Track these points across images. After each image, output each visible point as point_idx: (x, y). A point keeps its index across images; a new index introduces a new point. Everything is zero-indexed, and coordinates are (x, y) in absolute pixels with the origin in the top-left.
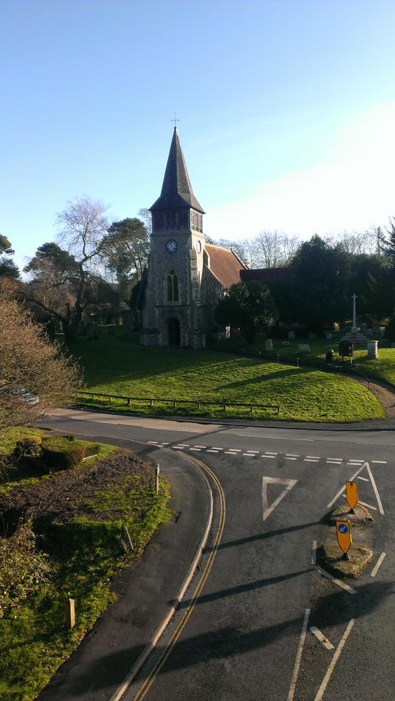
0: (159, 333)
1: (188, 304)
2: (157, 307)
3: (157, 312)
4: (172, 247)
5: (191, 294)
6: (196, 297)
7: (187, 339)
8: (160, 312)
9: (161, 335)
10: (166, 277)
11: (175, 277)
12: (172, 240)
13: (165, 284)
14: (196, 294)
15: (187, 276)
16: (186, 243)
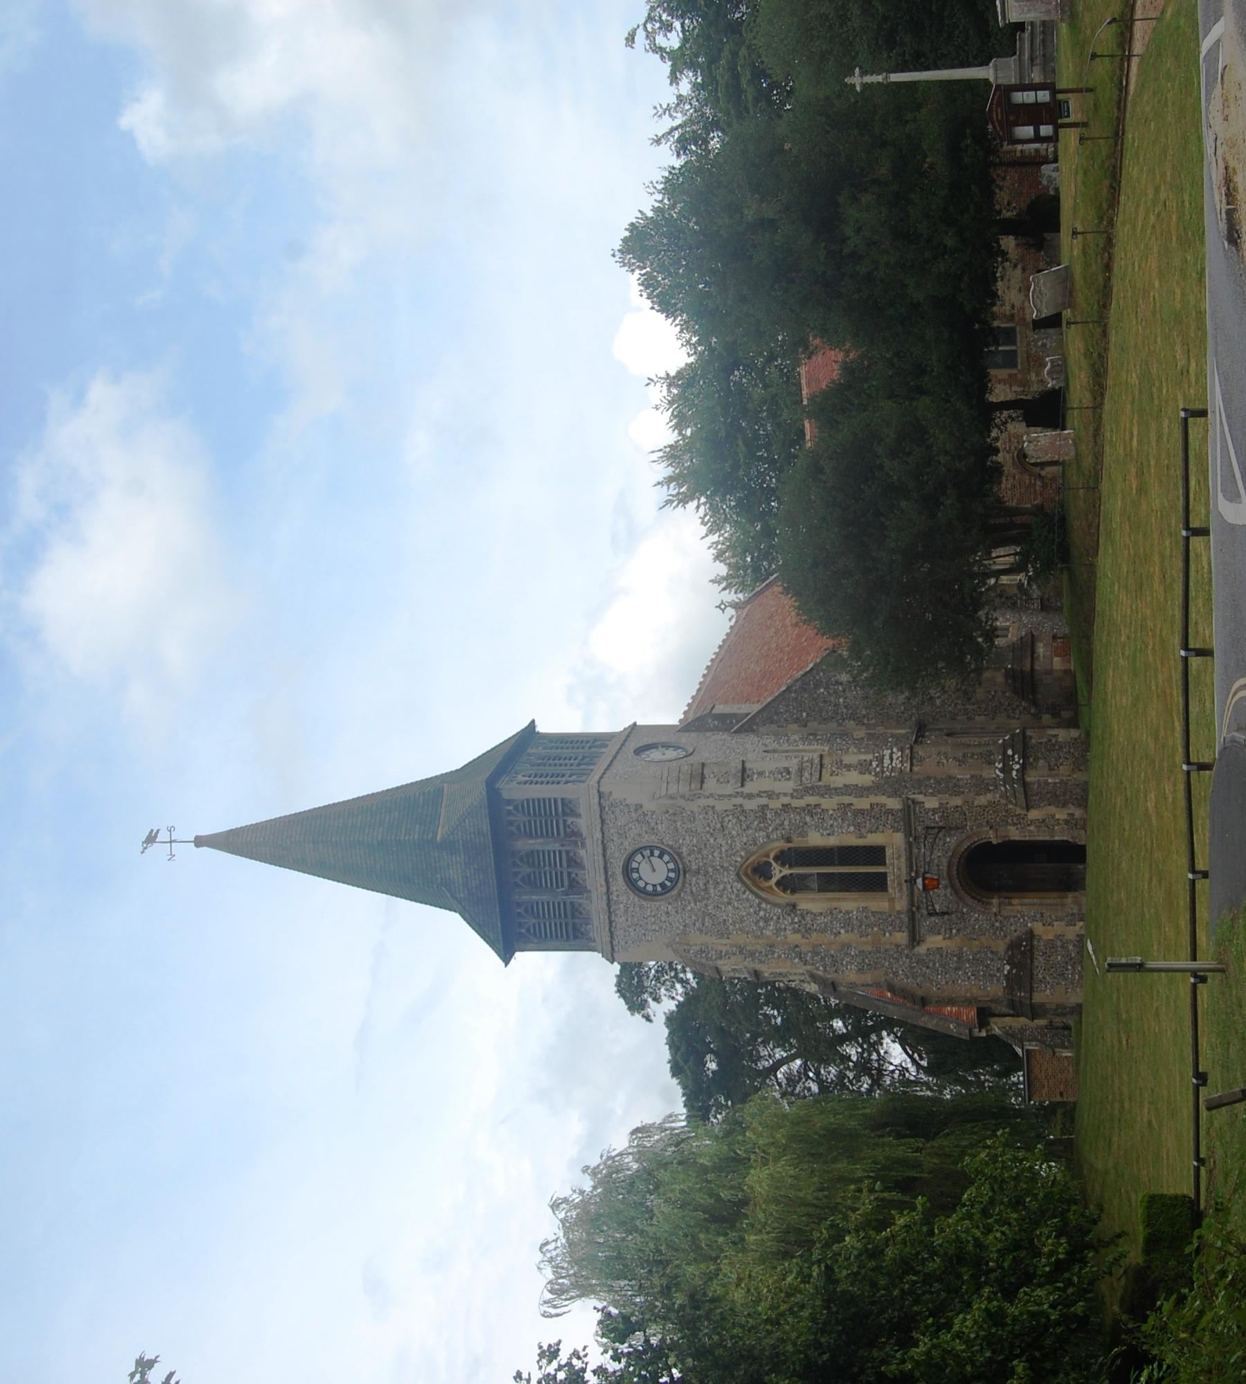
0: (1031, 935)
1: (894, 804)
2: (915, 940)
3: (934, 941)
4: (653, 872)
5: (847, 789)
6: (864, 767)
7: (1052, 809)
9: (1038, 928)
10: (787, 897)
11: (782, 858)
12: (627, 871)
14: (849, 767)
15: (775, 804)
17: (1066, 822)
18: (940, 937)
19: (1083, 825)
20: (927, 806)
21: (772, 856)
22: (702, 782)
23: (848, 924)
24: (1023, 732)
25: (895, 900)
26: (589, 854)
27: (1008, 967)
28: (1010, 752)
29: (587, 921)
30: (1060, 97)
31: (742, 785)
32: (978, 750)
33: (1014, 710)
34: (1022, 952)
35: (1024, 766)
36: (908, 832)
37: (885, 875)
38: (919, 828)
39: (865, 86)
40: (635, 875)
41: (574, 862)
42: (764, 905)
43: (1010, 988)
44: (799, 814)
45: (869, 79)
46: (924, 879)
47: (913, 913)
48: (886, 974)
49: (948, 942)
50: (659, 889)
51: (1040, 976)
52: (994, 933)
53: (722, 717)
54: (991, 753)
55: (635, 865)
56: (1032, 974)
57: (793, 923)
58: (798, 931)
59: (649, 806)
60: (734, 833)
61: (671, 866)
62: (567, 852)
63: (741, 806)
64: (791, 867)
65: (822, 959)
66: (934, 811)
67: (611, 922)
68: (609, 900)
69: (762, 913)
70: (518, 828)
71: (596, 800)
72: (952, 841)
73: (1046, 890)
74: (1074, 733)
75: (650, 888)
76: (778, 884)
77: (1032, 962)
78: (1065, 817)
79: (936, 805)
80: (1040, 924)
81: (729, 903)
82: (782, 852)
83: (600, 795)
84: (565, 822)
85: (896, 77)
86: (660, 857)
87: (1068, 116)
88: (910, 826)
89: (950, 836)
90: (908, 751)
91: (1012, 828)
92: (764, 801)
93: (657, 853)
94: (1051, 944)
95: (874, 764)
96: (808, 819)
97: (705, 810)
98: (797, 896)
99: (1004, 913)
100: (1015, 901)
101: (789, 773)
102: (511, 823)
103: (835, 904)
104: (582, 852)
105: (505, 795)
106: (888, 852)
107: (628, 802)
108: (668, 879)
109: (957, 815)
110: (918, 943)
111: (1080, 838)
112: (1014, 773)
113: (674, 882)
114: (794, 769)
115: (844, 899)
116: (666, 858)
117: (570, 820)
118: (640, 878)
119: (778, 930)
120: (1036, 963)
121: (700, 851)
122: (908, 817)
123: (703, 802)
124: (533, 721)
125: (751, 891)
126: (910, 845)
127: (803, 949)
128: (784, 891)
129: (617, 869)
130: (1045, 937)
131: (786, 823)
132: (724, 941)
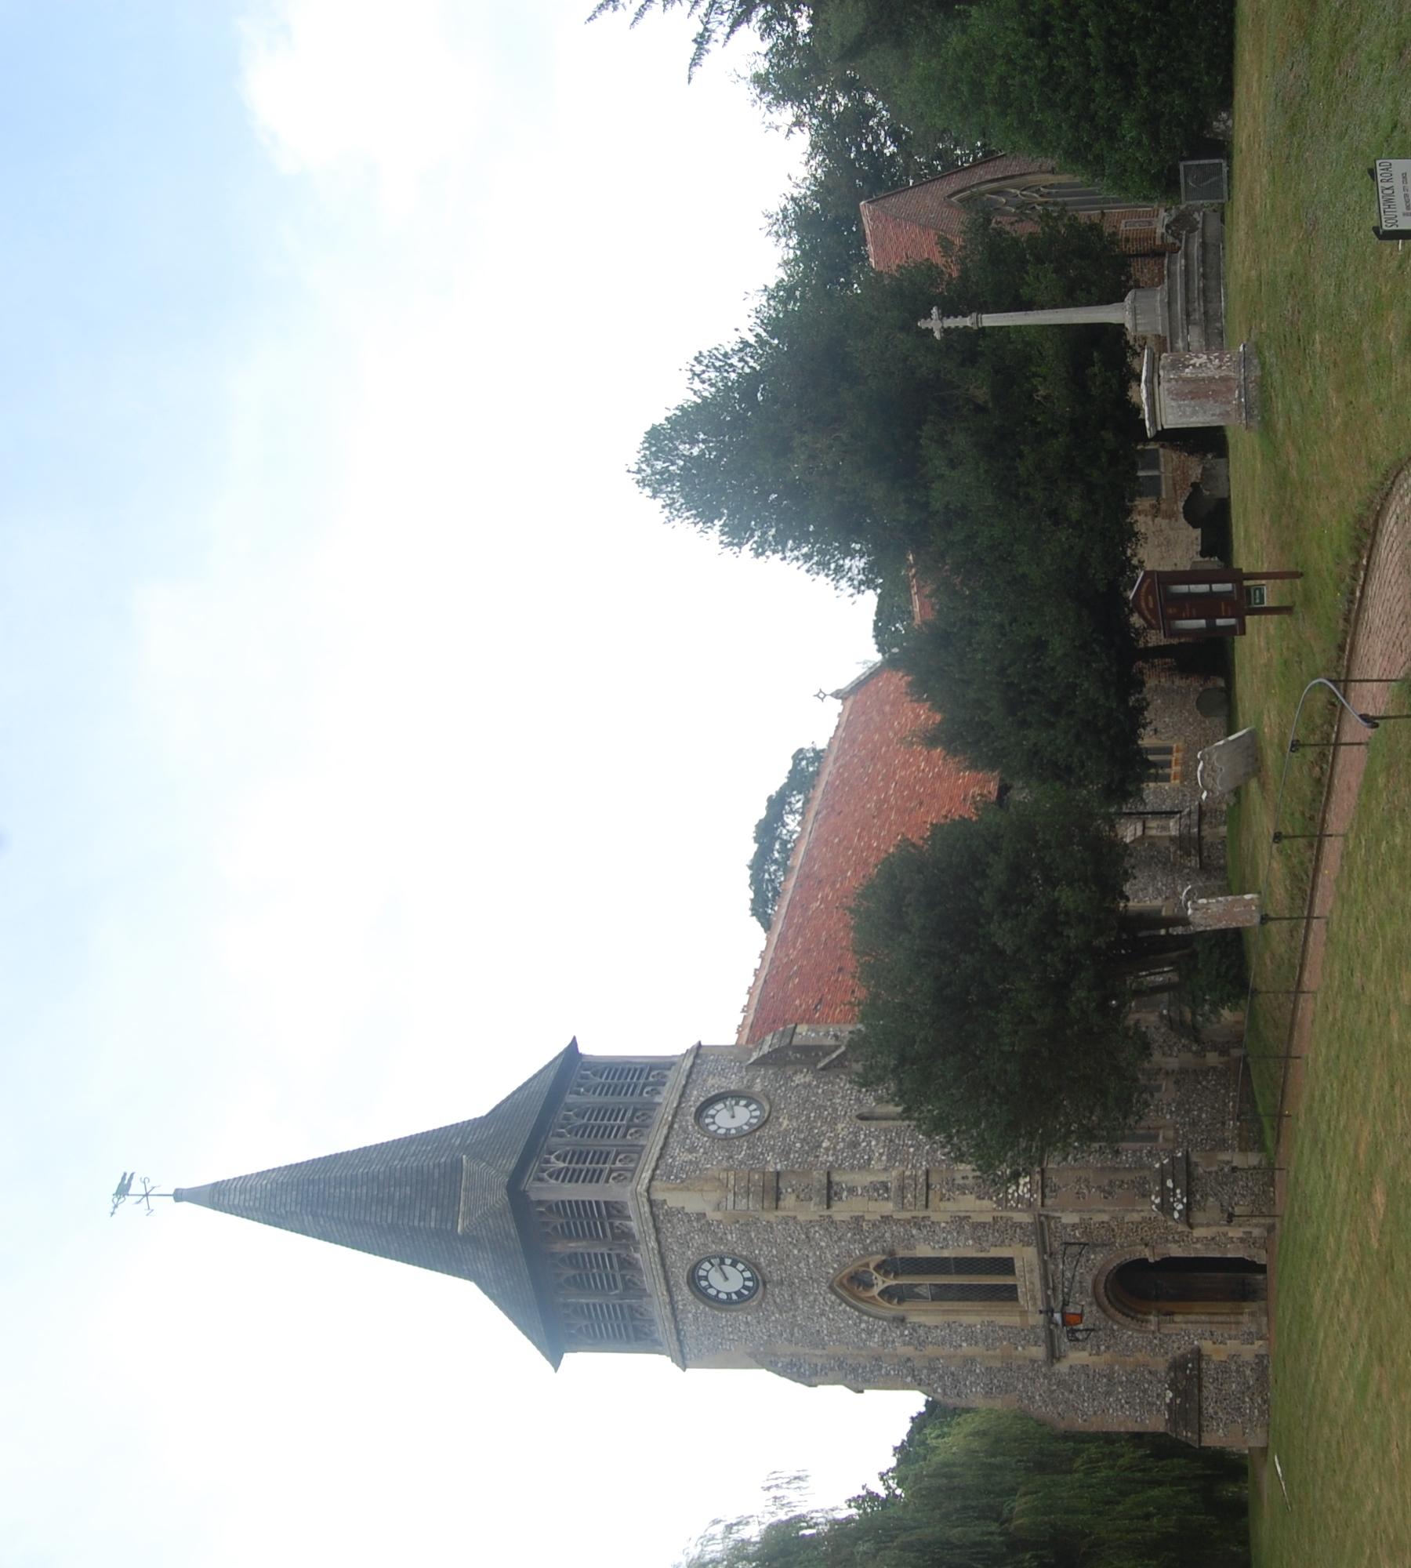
0: (1198, 1355)
1: (1024, 1218)
2: (1054, 1356)
3: (1077, 1356)
9: (1207, 1346)
10: (893, 1309)
12: (693, 1280)
13: (926, 1316)
16: (701, 1216)
17: (1242, 1240)
18: (1086, 1354)
19: (1266, 1244)
20: (1064, 1221)
21: (872, 1266)
22: (778, 1199)
23: (971, 1338)
24: (1187, 1156)
25: (1028, 1313)
26: (645, 1256)
27: (1170, 1394)
30: (1246, 583)
31: (829, 1207)
32: (1128, 1177)
33: (1170, 1047)
34: (1188, 1374)
35: (1188, 1207)
36: (1043, 1249)
37: (1014, 1287)
39: (946, 331)
40: (704, 1283)
41: (627, 1264)
42: (865, 1318)
43: (1172, 1421)
44: (903, 1226)
45: (952, 322)
46: (1064, 1315)
47: (1051, 1332)
48: (1021, 1399)
49: (1094, 1358)
50: (734, 1297)
51: (1211, 1411)
52: (1153, 1350)
53: (806, 1050)
54: (1145, 1181)
55: (702, 1273)
56: (1200, 1408)
57: (902, 1335)
58: (910, 1344)
59: (713, 1215)
61: (747, 1274)
62: (618, 1256)
64: (896, 1275)
65: (941, 1377)
66: (1074, 1226)
67: (678, 1332)
68: (674, 1309)
69: (863, 1325)
70: (555, 1228)
71: (647, 1208)
72: (1097, 1258)
73: (1217, 1300)
75: (723, 1296)
76: (882, 1293)
77: (1200, 1391)
78: (1241, 1235)
80: (1210, 1343)
81: (823, 1314)
83: (651, 1203)
84: (611, 1224)
85: (990, 320)
86: (734, 1265)
87: (1262, 602)
88: (1044, 1243)
89: (1095, 1253)
90: (1038, 1177)
93: (728, 1261)
94: (1223, 1368)
96: (914, 1232)
97: (785, 1221)
98: (906, 1306)
99: (1165, 1331)
101: (887, 1190)
102: (546, 1224)
103: (952, 1318)
104: (637, 1256)
105: (534, 1197)
106: (1018, 1264)
108: (744, 1287)
109: (1102, 1232)
110: (1059, 1359)
111: (1262, 1258)
112: (1176, 1215)
113: (753, 1291)
115: (966, 1312)
116: (740, 1267)
117: (617, 1223)
118: (711, 1286)
119: (884, 1344)
120: (1205, 1393)
121: (781, 1262)
122: (1041, 1232)
123: (780, 1213)
125: (848, 1304)
126: (1045, 1263)
129: (680, 1275)
130: (1215, 1358)
131: (887, 1235)
132: (818, 1352)
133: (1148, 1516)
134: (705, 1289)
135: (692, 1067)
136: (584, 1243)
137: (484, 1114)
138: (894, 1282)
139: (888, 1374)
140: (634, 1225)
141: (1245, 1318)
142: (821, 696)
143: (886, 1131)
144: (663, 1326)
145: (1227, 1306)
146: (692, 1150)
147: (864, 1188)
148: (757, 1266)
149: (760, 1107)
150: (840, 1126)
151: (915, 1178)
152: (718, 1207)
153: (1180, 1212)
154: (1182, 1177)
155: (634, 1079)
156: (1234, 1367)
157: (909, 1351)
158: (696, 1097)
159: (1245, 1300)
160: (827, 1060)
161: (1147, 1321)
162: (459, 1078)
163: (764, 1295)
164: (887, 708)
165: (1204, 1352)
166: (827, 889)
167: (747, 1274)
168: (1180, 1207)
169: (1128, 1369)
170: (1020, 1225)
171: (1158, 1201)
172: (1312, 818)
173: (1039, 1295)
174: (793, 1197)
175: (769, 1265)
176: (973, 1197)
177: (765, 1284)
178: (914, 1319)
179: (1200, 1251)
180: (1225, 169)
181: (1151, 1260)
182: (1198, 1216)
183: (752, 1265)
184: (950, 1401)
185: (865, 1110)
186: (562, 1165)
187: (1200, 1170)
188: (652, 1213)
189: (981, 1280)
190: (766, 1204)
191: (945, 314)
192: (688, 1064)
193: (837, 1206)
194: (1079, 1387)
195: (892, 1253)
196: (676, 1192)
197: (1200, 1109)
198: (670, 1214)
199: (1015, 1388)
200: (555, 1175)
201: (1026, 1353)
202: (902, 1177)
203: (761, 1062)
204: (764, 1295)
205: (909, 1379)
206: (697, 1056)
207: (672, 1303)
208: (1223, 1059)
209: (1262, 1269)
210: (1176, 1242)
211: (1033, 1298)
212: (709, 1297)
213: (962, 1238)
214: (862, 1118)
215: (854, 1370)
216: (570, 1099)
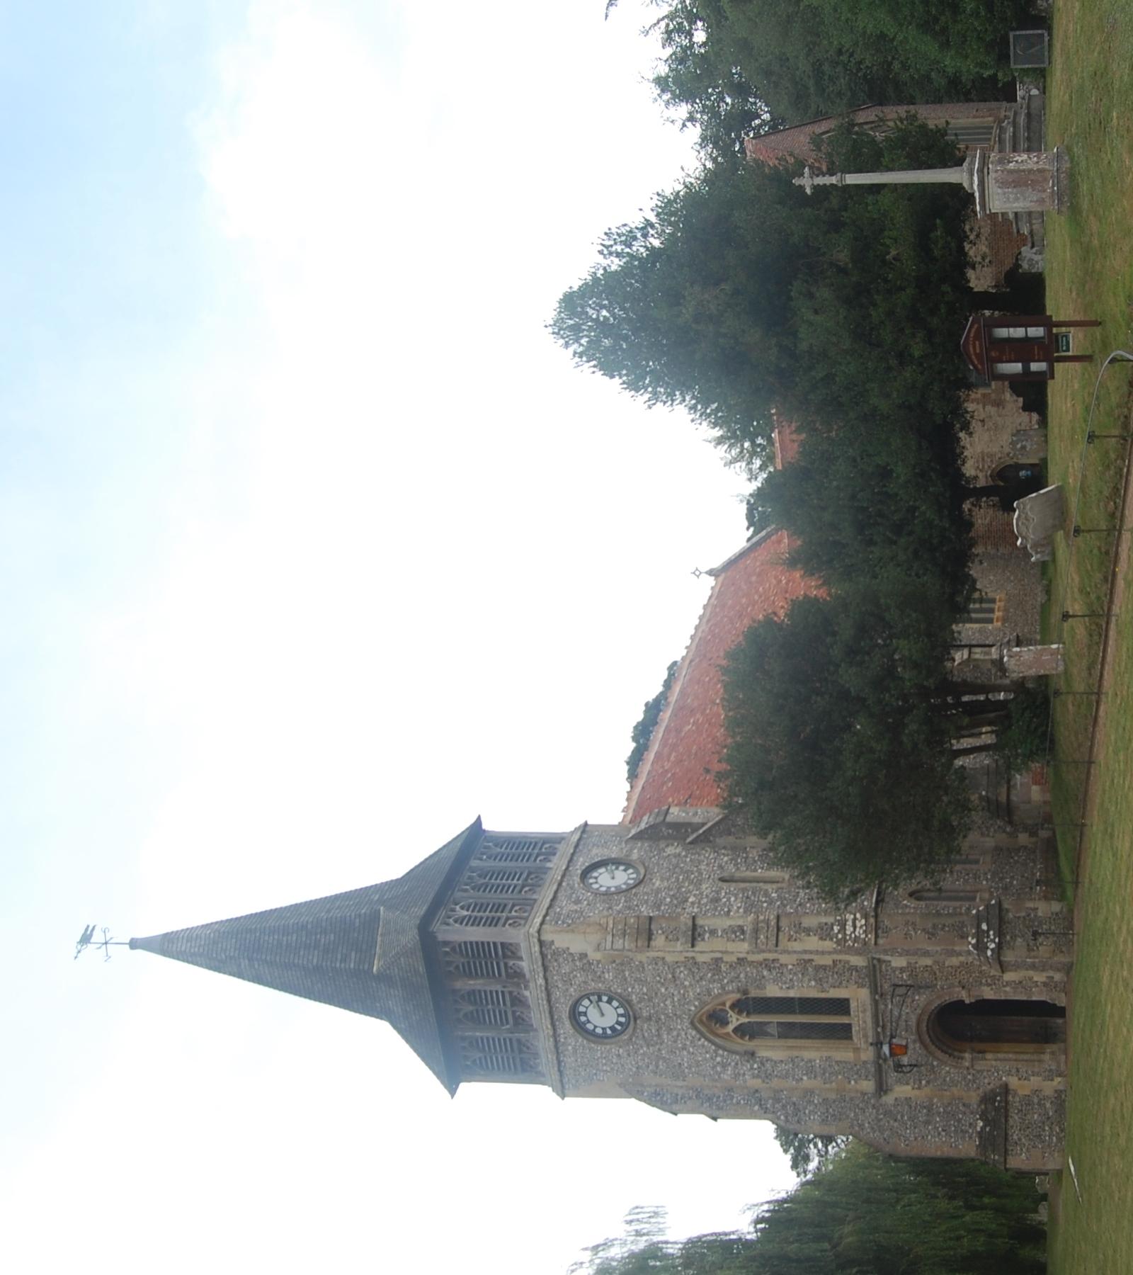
0: (1006, 1089)
1: (858, 961)
2: (882, 1089)
3: (902, 1090)
7: (1031, 973)
8: (899, 1081)
9: (1013, 1082)
11: (739, 1006)
12: (574, 1015)
13: (772, 1051)
14: (808, 931)
16: (583, 956)
17: (1045, 984)
18: (909, 1087)
19: (1066, 988)
20: (893, 964)
21: (728, 1004)
22: (650, 939)
23: (810, 1071)
24: (1000, 903)
26: (533, 993)
27: (981, 1124)
28: (984, 927)
29: (536, 1055)
30: (1055, 330)
31: (693, 946)
32: (949, 921)
33: (988, 829)
34: (996, 1106)
36: (874, 989)
37: (849, 1026)
38: (886, 986)
40: (583, 1019)
41: (518, 1001)
42: (720, 1052)
43: (982, 1147)
46: (890, 1044)
47: (880, 1066)
49: (917, 1092)
50: (609, 1032)
51: (1015, 1137)
52: (967, 1085)
53: (677, 826)
54: (963, 924)
55: (582, 1009)
56: (1006, 1134)
57: (752, 1068)
58: (758, 1076)
59: (594, 956)
60: (687, 983)
61: (621, 1011)
62: (510, 993)
63: (693, 958)
64: (748, 1014)
65: (784, 1107)
66: (902, 970)
67: (559, 1063)
68: (556, 1042)
69: (719, 1059)
70: (457, 967)
71: (537, 948)
72: (921, 999)
74: (1056, 907)
75: (599, 1031)
76: (736, 1030)
77: (1007, 1121)
78: (1044, 979)
79: (904, 964)
81: (684, 1048)
82: (739, 1001)
83: (541, 943)
84: (506, 964)
85: (852, 179)
86: (609, 1002)
87: (1068, 350)
89: (919, 994)
90: (872, 920)
91: (986, 989)
92: (719, 955)
93: (605, 998)
94: (1027, 1101)
95: (836, 929)
96: (765, 973)
97: (655, 961)
100: (989, 1056)
101: (743, 932)
102: (449, 963)
103: (795, 1053)
104: (527, 993)
105: (440, 937)
106: (853, 1005)
107: (572, 951)
108: (618, 1023)
109: (926, 975)
110: (886, 1092)
111: (1061, 1001)
112: (989, 953)
113: (625, 1026)
114: (748, 929)
116: (615, 1004)
117: (511, 963)
118: (589, 1022)
119: (736, 1076)
120: (1011, 1122)
121: (650, 1000)
122: (874, 975)
123: (652, 954)
124: (479, 818)
125: (707, 1039)
126: (876, 1003)
127: (764, 1095)
128: (742, 1037)
129: (563, 1010)
130: (1021, 1092)
132: (680, 1083)
133: (959, 1238)
134: (584, 1024)
135: (580, 840)
136: (481, 981)
137: (400, 876)
138: (747, 1020)
139: (738, 1103)
140: (525, 965)
141: (1047, 1057)
142: (697, 573)
143: (744, 890)
144: (546, 1059)
145: (1031, 1047)
146: (578, 902)
147: (724, 931)
148: (629, 1002)
149: (637, 871)
150: (704, 886)
151: (767, 922)
152: (598, 948)
153: (992, 950)
154: (995, 921)
155: (530, 852)
156: (1036, 1100)
157: (757, 1083)
158: (581, 863)
159: (1047, 1042)
160: (695, 835)
161: (963, 1058)
162: (381, 847)
163: (635, 1028)
164: (754, 579)
165: (1011, 1087)
166: (698, 716)
167: (621, 1011)
168: (993, 946)
169: (946, 1102)
170: (856, 968)
171: (974, 941)
172: (1107, 553)
173: (870, 1033)
174: (663, 937)
175: (639, 1002)
176: (816, 938)
177: (635, 1019)
178: (763, 1053)
179: (1009, 994)
180: (1046, 39)
181: (967, 1001)
182: (1009, 957)
183: (625, 1002)
184: (792, 1127)
185: (725, 874)
186: (465, 913)
187: (1011, 915)
188: (541, 952)
189: (819, 1019)
190: (640, 944)
191: (816, 172)
192: (576, 837)
193: (700, 946)
194: (902, 1116)
195: (745, 992)
196: (566, 933)
197: (1012, 878)
198: (557, 953)
199: (848, 1117)
200: (460, 921)
201: (858, 1087)
202: (757, 922)
203: (640, 836)
204: (635, 1028)
205: (756, 1108)
206: (583, 832)
207: (555, 1036)
208: (1034, 839)
209: (1060, 1012)
210: (989, 985)
211: (865, 1036)
212: (587, 1031)
213: (806, 979)
214: (723, 880)
215: (709, 1099)
216: (474, 863)
